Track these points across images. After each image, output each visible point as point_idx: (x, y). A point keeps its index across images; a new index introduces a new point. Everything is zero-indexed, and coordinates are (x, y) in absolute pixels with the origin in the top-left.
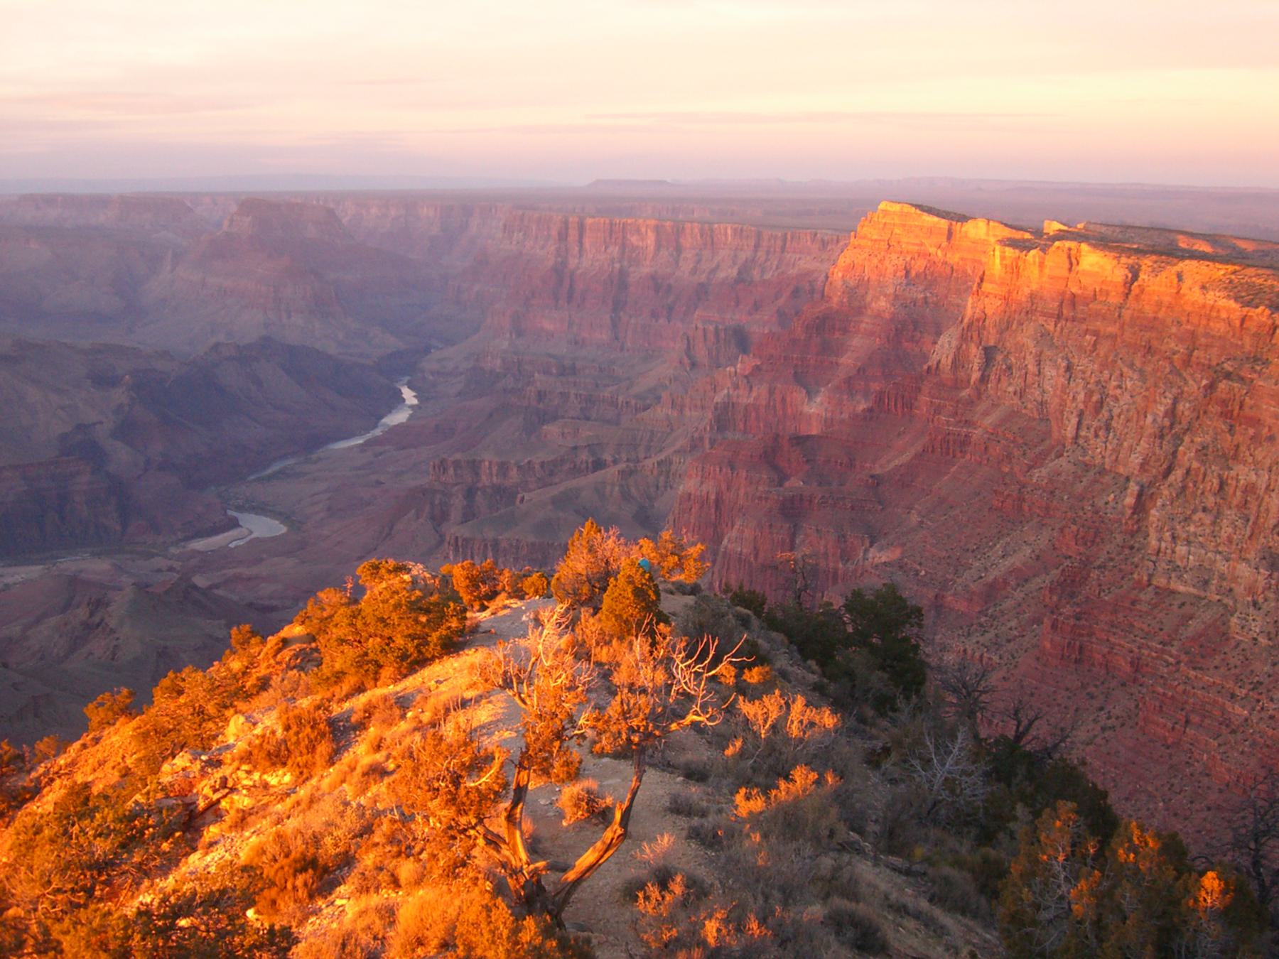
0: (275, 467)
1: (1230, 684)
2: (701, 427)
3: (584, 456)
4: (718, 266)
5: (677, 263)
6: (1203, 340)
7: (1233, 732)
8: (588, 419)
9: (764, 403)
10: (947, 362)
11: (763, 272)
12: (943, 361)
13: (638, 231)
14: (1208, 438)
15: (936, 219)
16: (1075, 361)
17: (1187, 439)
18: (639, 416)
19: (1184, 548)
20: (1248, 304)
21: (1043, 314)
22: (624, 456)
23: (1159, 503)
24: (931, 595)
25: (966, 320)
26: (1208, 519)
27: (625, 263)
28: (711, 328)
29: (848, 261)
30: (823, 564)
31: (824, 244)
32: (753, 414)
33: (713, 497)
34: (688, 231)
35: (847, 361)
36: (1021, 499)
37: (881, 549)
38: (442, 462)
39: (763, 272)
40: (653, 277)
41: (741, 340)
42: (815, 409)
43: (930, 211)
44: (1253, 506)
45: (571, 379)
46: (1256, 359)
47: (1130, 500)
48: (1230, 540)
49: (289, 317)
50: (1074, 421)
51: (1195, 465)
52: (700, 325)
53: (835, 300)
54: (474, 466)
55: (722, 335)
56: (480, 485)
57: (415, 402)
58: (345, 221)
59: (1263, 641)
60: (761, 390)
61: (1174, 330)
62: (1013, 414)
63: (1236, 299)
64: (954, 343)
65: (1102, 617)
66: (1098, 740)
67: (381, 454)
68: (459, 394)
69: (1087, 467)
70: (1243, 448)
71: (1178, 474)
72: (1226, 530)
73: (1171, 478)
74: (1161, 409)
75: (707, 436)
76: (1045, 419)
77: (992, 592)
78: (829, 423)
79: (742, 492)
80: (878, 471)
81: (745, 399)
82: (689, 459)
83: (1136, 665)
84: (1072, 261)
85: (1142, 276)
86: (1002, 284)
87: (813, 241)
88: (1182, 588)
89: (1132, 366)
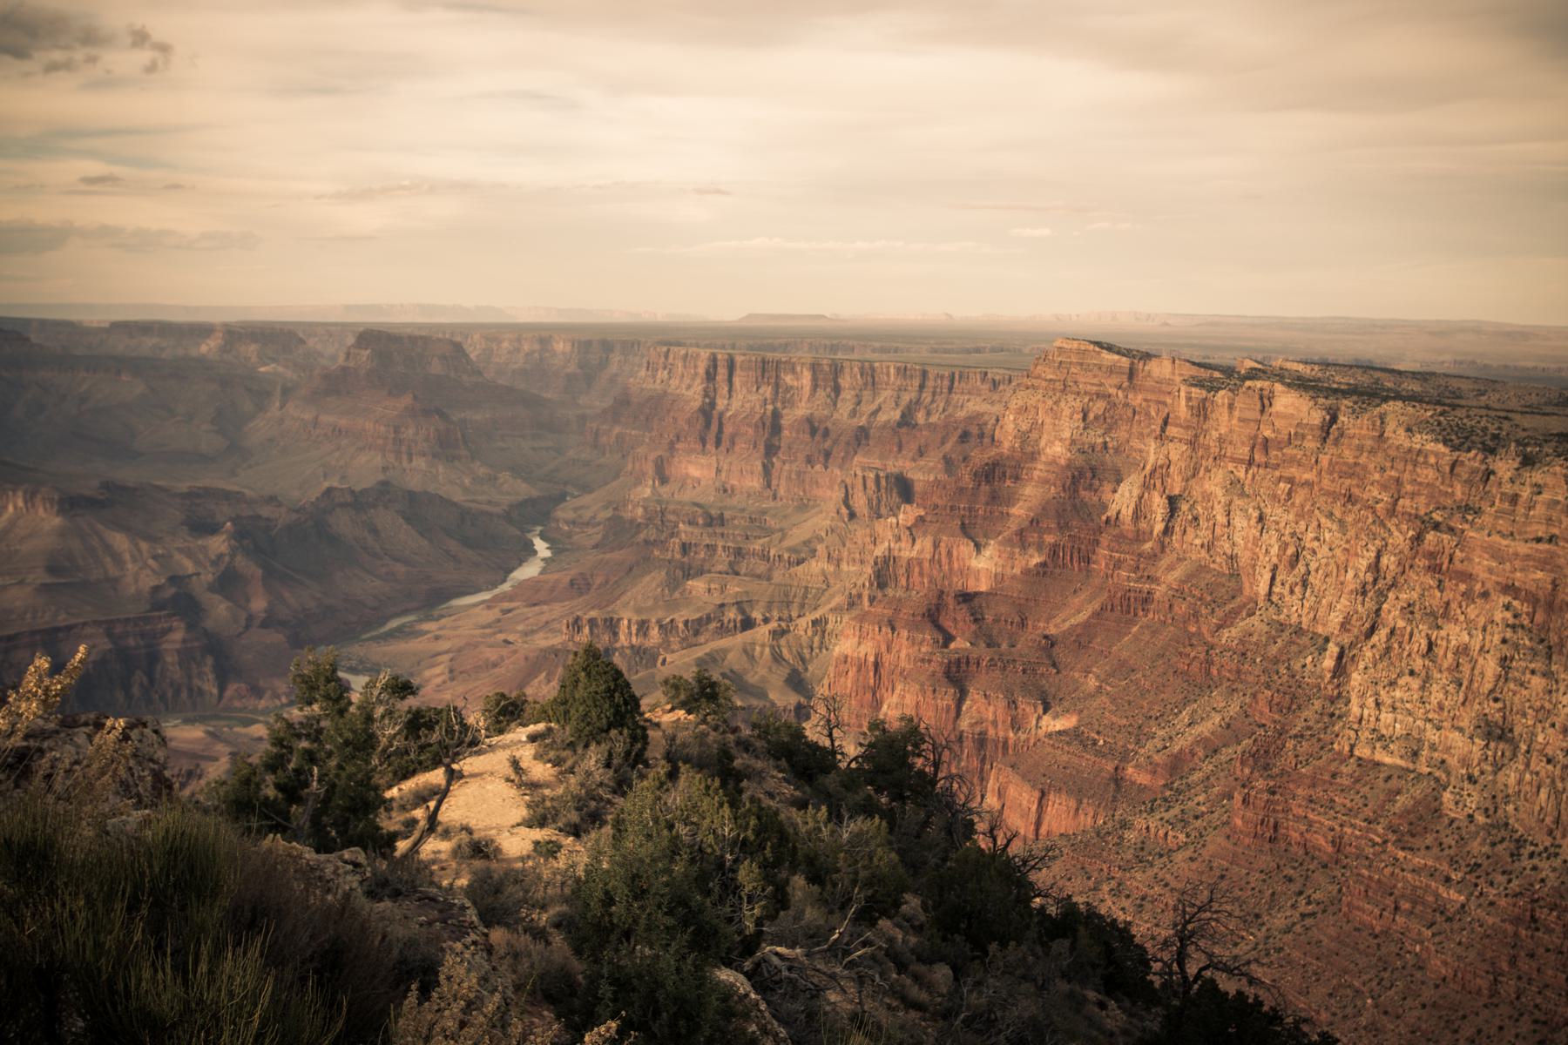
0: (394, 624)
1: (1444, 867)
2: (860, 583)
3: (732, 614)
4: (879, 409)
5: (835, 405)
6: (1409, 488)
7: (1449, 920)
8: (737, 574)
9: (928, 557)
10: (1127, 513)
11: (928, 414)
12: (1124, 511)
13: (793, 370)
14: (1415, 595)
15: (1116, 357)
16: (1268, 511)
17: (1391, 595)
18: (792, 570)
19: (1391, 716)
20: (1455, 448)
21: (1233, 460)
22: (776, 614)
23: (1361, 666)
24: (1110, 767)
25: (1148, 468)
26: (1415, 683)
27: (779, 405)
28: (872, 475)
29: (1020, 403)
30: (991, 732)
31: (995, 385)
32: (917, 570)
33: (871, 659)
34: (847, 370)
35: (1019, 511)
36: (1210, 663)
37: (1056, 717)
38: (577, 619)
39: (928, 414)
40: (809, 420)
41: (904, 489)
42: (984, 565)
43: (1110, 348)
44: (1466, 669)
45: (719, 530)
46: (1468, 508)
47: (1329, 663)
48: (1441, 707)
49: (410, 460)
50: (1267, 576)
51: (1401, 624)
52: (859, 473)
53: (1006, 444)
54: (612, 625)
55: (883, 483)
56: (618, 645)
57: (548, 554)
58: (473, 356)
59: (1480, 819)
60: (924, 545)
61: (1377, 476)
62: (1201, 568)
63: (1445, 442)
64: (1136, 492)
65: (1300, 791)
66: (1298, 928)
67: (509, 611)
68: (596, 546)
69: (1282, 627)
70: (1454, 605)
71: (1380, 636)
72: (1436, 696)
73: (1375, 639)
74: (1363, 564)
75: (866, 593)
76: (1235, 575)
77: (1177, 765)
78: (999, 578)
79: (903, 654)
80: (1052, 631)
81: (906, 552)
82: (846, 618)
83: (1338, 844)
84: (1266, 400)
85: (1342, 418)
86: (1188, 428)
87: (983, 380)
88: (1388, 760)
89: (1330, 515)
